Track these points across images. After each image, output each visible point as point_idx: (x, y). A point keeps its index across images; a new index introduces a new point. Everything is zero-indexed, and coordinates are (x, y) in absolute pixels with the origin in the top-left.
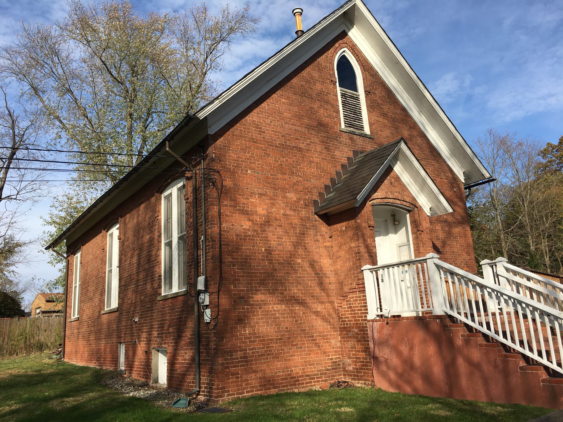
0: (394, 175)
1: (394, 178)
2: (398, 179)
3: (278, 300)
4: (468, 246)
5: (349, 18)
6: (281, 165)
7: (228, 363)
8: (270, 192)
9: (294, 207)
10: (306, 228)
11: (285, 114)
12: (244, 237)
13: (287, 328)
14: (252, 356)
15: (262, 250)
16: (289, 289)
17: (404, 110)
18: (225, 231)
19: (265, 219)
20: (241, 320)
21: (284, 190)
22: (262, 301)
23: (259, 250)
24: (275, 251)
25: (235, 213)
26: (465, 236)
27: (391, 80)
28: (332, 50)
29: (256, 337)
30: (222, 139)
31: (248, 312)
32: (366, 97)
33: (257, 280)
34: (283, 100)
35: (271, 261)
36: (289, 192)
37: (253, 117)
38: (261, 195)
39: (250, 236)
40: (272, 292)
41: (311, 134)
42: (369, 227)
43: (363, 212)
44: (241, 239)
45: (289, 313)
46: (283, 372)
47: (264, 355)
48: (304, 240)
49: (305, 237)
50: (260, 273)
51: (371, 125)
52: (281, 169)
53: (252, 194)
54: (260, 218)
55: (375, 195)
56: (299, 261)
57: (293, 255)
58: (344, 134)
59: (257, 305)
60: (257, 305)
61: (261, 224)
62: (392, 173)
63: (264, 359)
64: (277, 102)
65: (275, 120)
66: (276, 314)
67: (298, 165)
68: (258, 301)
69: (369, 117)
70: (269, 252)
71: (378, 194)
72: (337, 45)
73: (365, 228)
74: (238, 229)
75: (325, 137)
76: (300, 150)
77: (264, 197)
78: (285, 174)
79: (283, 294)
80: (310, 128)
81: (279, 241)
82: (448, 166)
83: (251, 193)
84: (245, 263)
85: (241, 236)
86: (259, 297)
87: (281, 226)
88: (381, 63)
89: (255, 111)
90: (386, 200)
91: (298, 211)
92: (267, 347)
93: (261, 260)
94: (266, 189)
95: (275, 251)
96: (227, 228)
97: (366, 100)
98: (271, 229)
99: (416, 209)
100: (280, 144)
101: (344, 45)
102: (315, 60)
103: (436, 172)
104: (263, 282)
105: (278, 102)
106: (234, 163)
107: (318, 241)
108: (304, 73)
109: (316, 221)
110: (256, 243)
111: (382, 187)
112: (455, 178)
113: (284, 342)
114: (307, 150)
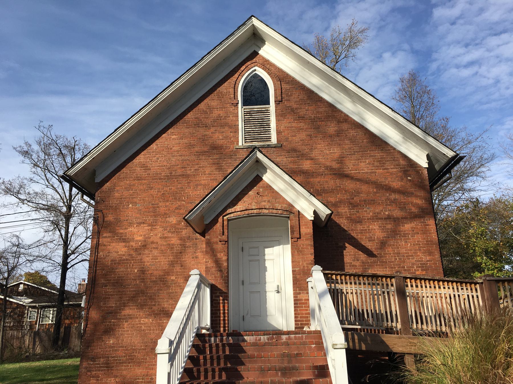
0: (264, 184)
1: (262, 187)
2: (269, 188)
3: (146, 315)
4: (429, 243)
5: (256, 38)
6: (163, 194)
7: (90, 368)
8: (150, 219)
9: (175, 229)
10: (185, 247)
11: (173, 148)
12: (121, 262)
13: (152, 340)
14: (113, 363)
15: (134, 271)
16: (158, 305)
17: (331, 106)
18: (101, 259)
19: (141, 244)
20: (109, 331)
21: (165, 215)
22: (129, 315)
23: (131, 271)
24: (148, 271)
25: (112, 242)
26: (425, 232)
27: (312, 81)
28: (236, 75)
29: (120, 347)
30: (108, 184)
31: (114, 325)
32: (276, 107)
33: (127, 297)
34: (174, 137)
35: (143, 280)
36: (169, 217)
37: (141, 158)
38: (139, 224)
39: (124, 260)
40: (141, 306)
41: (200, 159)
42: (220, 241)
43: (215, 227)
44: (115, 264)
45: (155, 326)
46: (142, 379)
47: (126, 363)
48: (180, 258)
49: (182, 256)
50: (130, 291)
51: (278, 133)
52: (164, 197)
53: (131, 224)
54: (136, 244)
55: (230, 211)
56: (173, 278)
57: (167, 273)
58: (241, 151)
59: (123, 319)
60: (123, 319)
61: (136, 249)
62: (261, 183)
63: (125, 366)
64: (167, 140)
65: (162, 156)
66: (141, 327)
67: (182, 191)
68: (125, 315)
69: (277, 126)
70: (143, 271)
71: (239, 207)
72: (242, 69)
73: (217, 243)
74: (114, 255)
75: (217, 159)
76: (188, 176)
77: (142, 225)
78: (167, 201)
79: (152, 308)
80: (200, 155)
81: (155, 261)
82: (400, 153)
83: (130, 223)
84: (119, 283)
85: (116, 261)
86: (127, 311)
87: (157, 248)
88: (297, 65)
89: (142, 153)
90: (247, 212)
91: (177, 232)
92: (129, 356)
93: (133, 279)
94: (145, 218)
95: (148, 271)
96: (103, 255)
97: (276, 110)
98: (147, 252)
99: (292, 215)
100: (164, 176)
101: (253, 65)
102: (216, 89)
103: (376, 164)
104: (133, 298)
105: (171, 139)
106: (117, 201)
107: (197, 257)
108: (202, 106)
109: (196, 239)
110: (130, 265)
111: (245, 199)
112: (412, 164)
113: (147, 352)
114: (194, 175)
